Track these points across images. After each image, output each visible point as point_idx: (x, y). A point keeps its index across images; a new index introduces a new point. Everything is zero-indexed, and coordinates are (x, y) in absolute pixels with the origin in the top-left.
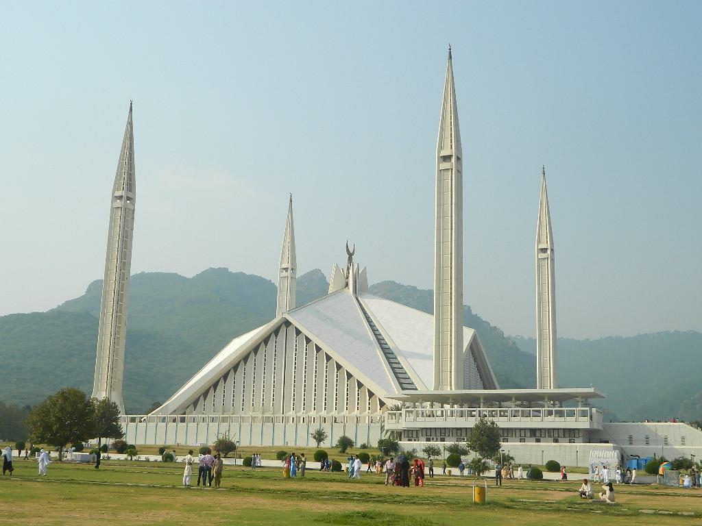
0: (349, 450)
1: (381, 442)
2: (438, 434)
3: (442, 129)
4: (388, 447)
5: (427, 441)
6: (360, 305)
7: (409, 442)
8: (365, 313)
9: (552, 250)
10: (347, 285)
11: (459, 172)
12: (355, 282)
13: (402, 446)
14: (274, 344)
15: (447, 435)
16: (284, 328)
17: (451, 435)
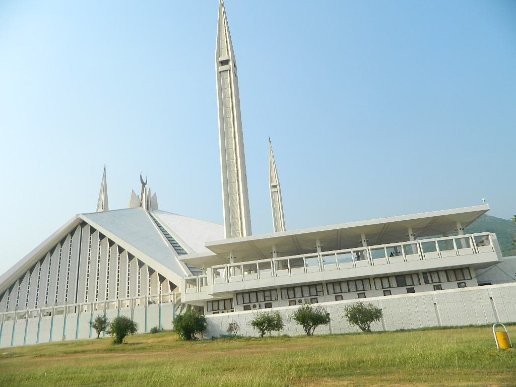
0: (129, 338)
1: (178, 320)
2: (261, 298)
3: (219, 43)
4: (191, 326)
5: (245, 310)
6: (152, 217)
7: (216, 315)
8: (156, 222)
9: (279, 186)
10: (141, 205)
11: (236, 76)
12: (147, 202)
13: (215, 322)
14: (70, 243)
15: (273, 299)
16: (79, 228)
17: (279, 298)
